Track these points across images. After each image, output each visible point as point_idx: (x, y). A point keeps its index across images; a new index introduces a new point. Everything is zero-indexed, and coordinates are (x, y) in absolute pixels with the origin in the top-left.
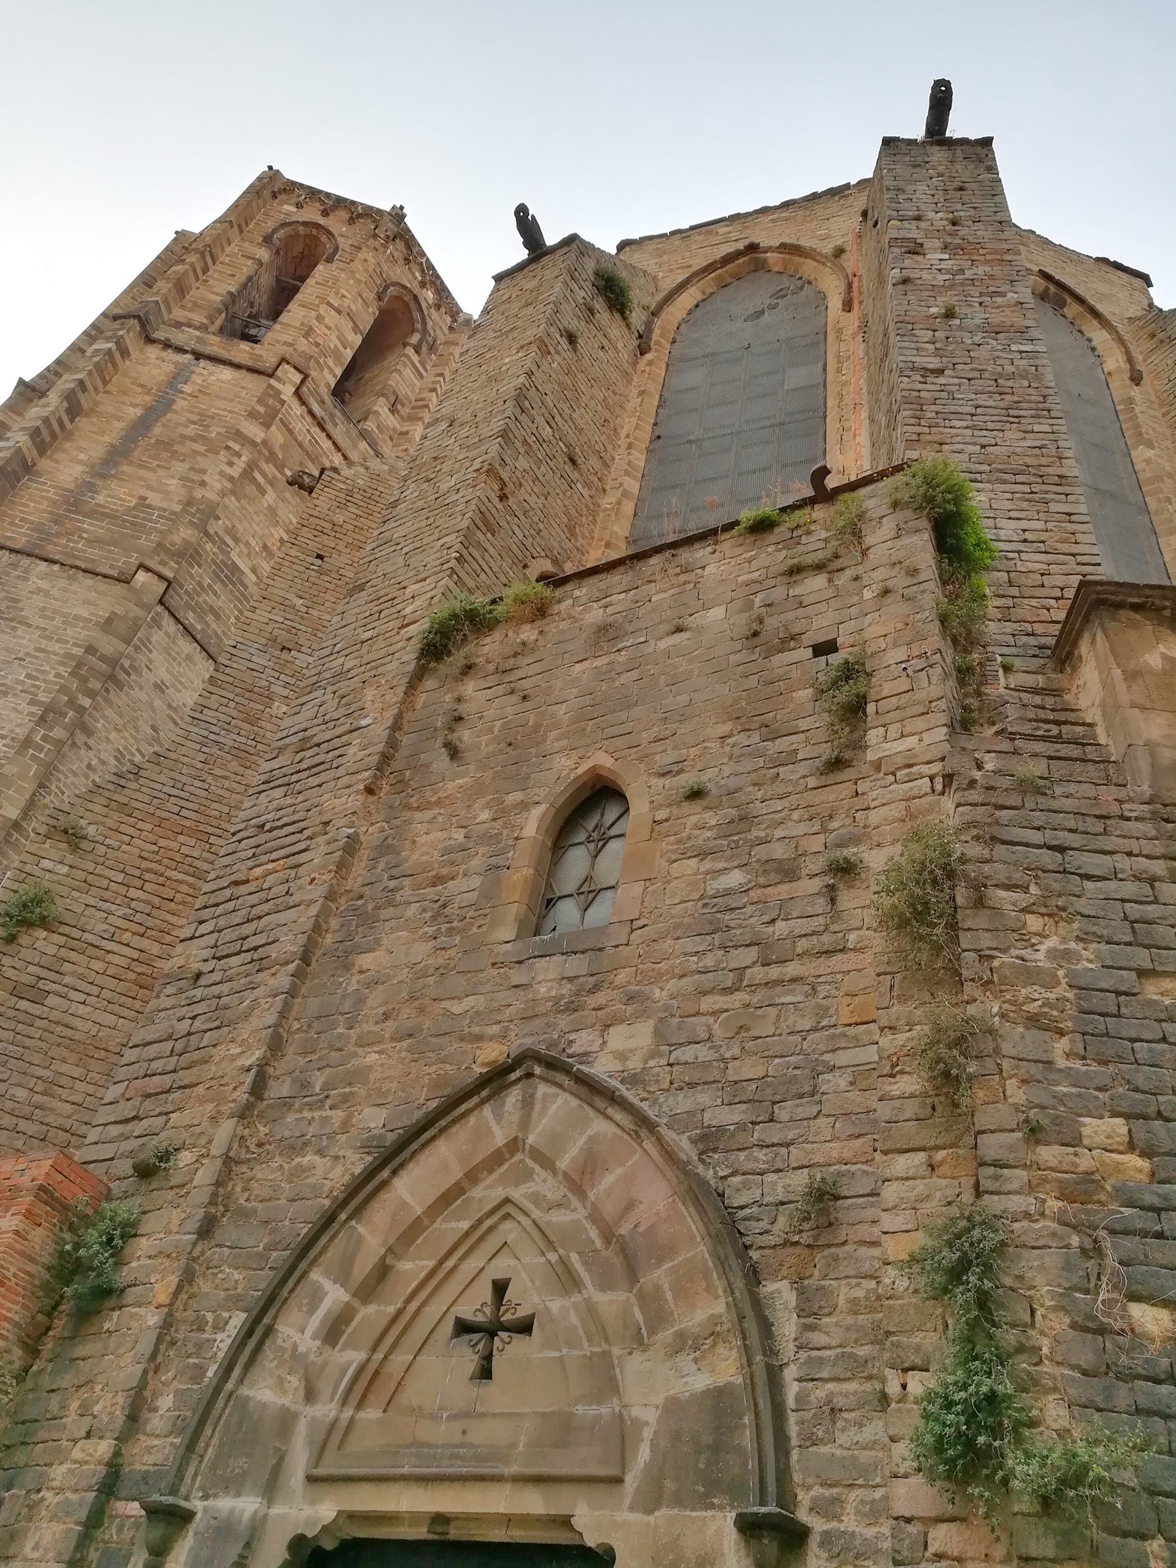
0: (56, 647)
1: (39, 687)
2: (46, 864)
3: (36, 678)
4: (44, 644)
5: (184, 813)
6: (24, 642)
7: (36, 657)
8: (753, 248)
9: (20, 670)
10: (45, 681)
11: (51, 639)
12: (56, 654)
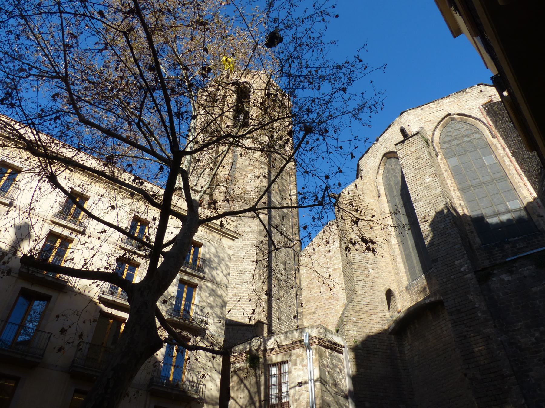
0: (248, 243)
1: (250, 256)
2: (351, 332)
3: (248, 254)
4: (245, 242)
5: (370, 308)
6: (240, 243)
7: (245, 247)
8: (449, 114)
9: (243, 252)
10: (251, 254)
11: (245, 240)
12: (249, 245)
